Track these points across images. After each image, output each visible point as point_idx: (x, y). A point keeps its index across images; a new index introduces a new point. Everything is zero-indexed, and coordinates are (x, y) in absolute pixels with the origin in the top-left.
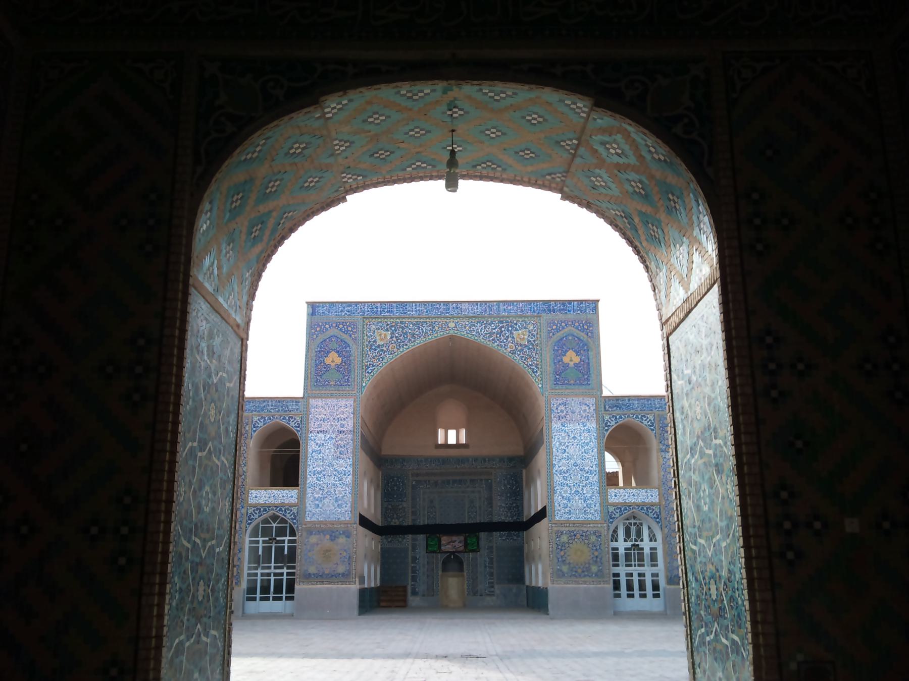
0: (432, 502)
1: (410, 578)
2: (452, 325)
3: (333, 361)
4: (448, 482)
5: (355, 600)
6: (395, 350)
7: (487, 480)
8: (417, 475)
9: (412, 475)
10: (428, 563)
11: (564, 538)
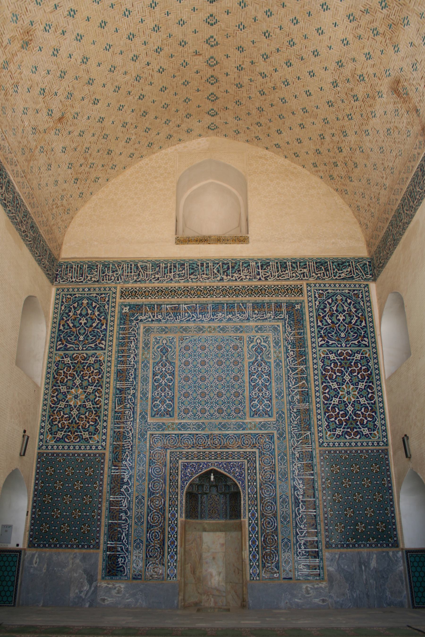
0: (164, 351)
1: (103, 530)
4: (203, 308)
7: (290, 305)
9: (123, 295)
10: (151, 493)
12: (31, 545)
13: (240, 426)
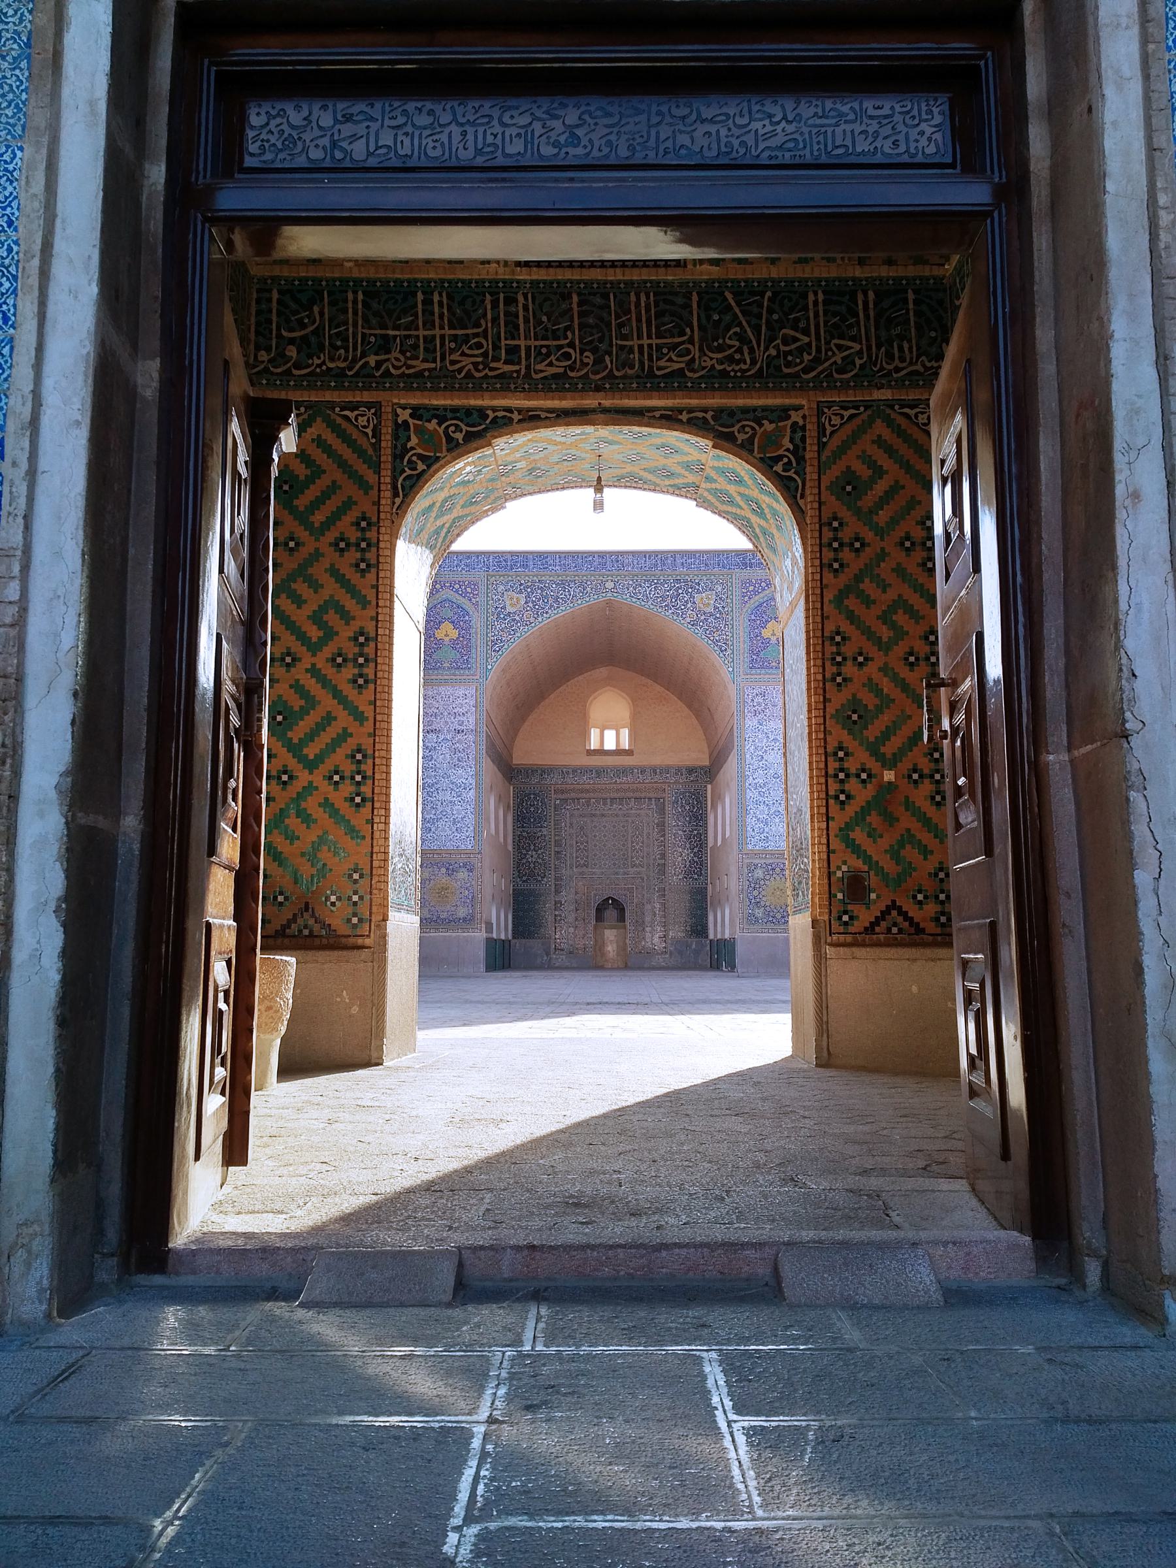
0: (582, 828)
2: (610, 585)
3: (447, 635)
5: (481, 954)
6: (532, 620)
8: (563, 792)
11: (759, 873)
12: (514, 938)
13: (625, 873)
